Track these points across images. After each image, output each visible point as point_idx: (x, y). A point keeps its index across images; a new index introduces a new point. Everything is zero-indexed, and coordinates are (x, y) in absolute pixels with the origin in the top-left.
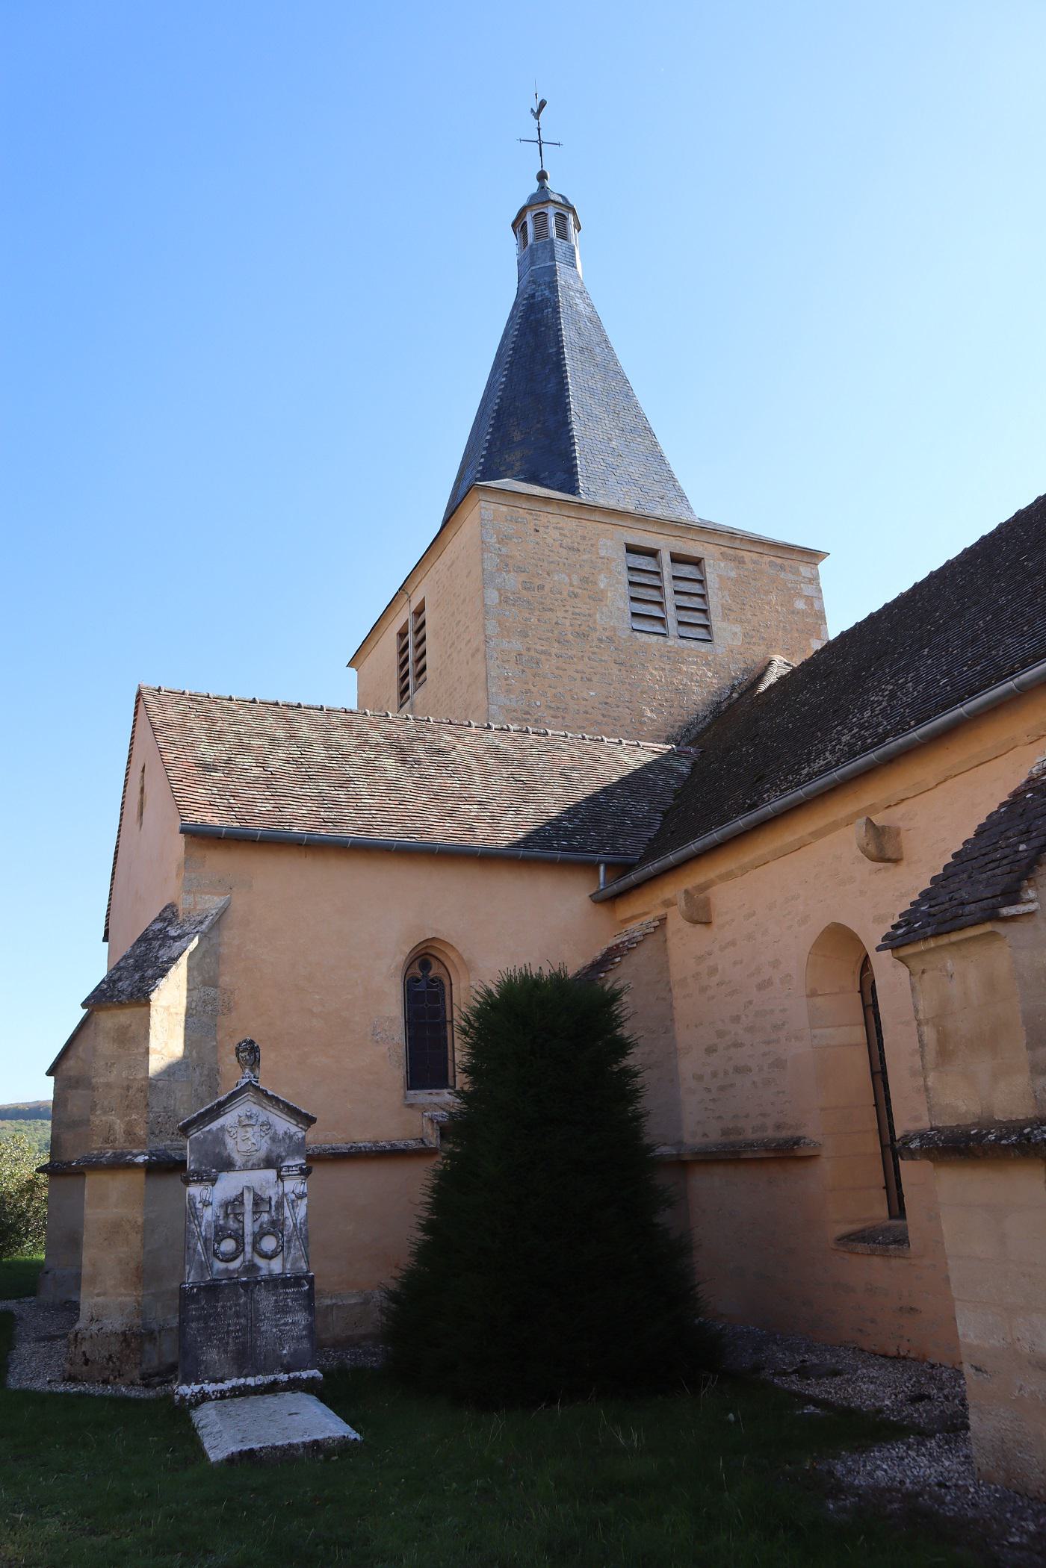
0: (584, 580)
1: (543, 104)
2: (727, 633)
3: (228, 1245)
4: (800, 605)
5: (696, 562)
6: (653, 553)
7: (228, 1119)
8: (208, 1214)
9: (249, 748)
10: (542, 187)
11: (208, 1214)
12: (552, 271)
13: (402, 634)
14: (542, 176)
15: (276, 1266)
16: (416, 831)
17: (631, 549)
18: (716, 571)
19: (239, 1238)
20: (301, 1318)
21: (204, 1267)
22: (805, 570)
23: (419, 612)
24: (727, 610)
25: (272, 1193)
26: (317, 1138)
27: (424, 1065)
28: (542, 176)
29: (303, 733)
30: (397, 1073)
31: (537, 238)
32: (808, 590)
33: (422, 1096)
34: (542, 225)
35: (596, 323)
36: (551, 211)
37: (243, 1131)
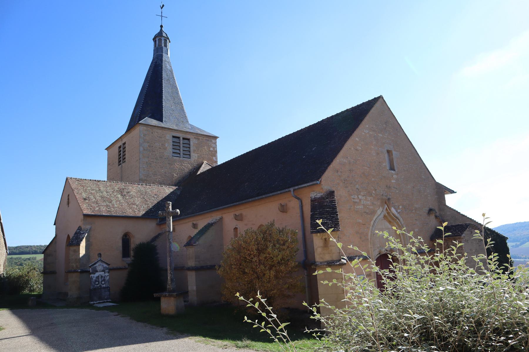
0: (162, 145)
1: (163, 6)
2: (194, 156)
3: (97, 283)
4: (211, 149)
5: (189, 139)
6: (179, 138)
7: (97, 265)
8: (94, 278)
9: (91, 193)
10: (161, 30)
11: (94, 278)
12: (162, 56)
13: (120, 147)
14: (161, 26)
15: (104, 286)
16: (125, 213)
17: (174, 137)
18: (193, 142)
19: (99, 282)
20: (108, 293)
21: (94, 286)
22: (213, 141)
25: (104, 275)
27: (126, 252)
28: (161, 26)
29: (102, 189)
30: (121, 255)
31: (159, 46)
32: (213, 145)
33: (125, 259)
34: (160, 41)
35: (171, 71)
36: (163, 39)
37: (99, 266)
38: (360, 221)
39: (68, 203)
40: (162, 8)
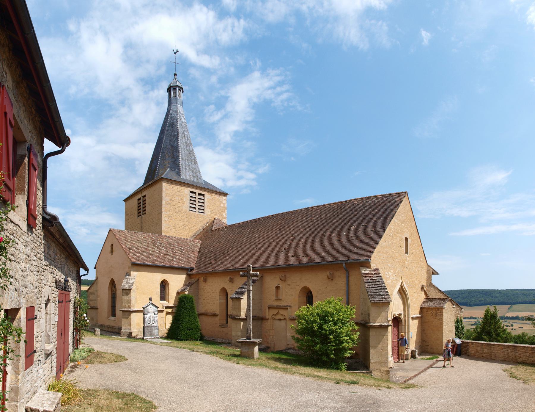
0: (181, 199)
4: (222, 205)
5: (203, 195)
6: (195, 193)
26: (159, 309)
33: (162, 302)
39: (112, 252)
40: (175, 53)
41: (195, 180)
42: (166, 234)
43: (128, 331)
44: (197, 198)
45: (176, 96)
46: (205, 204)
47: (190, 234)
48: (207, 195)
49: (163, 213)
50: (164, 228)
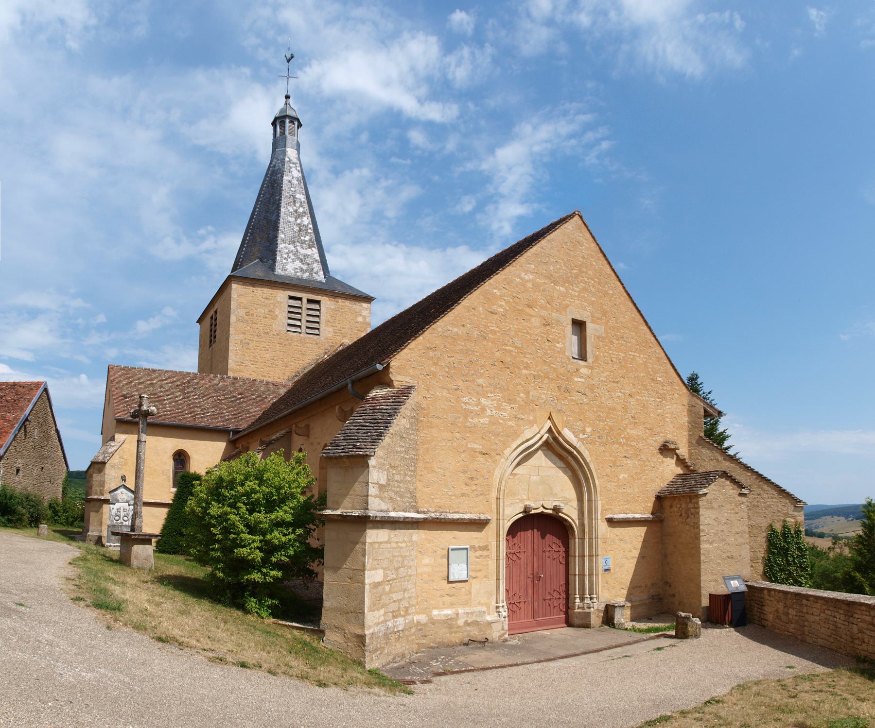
4: (360, 319)
5: (318, 302)
6: (300, 299)
7: (119, 492)
17: (291, 298)
23: (216, 312)
24: (328, 321)
38: (476, 446)
41: (306, 276)
42: (236, 375)
43: (97, 534)
44: (304, 308)
45: (284, 134)
46: (322, 317)
47: (288, 374)
48: (327, 303)
49: (231, 338)
50: (232, 363)
